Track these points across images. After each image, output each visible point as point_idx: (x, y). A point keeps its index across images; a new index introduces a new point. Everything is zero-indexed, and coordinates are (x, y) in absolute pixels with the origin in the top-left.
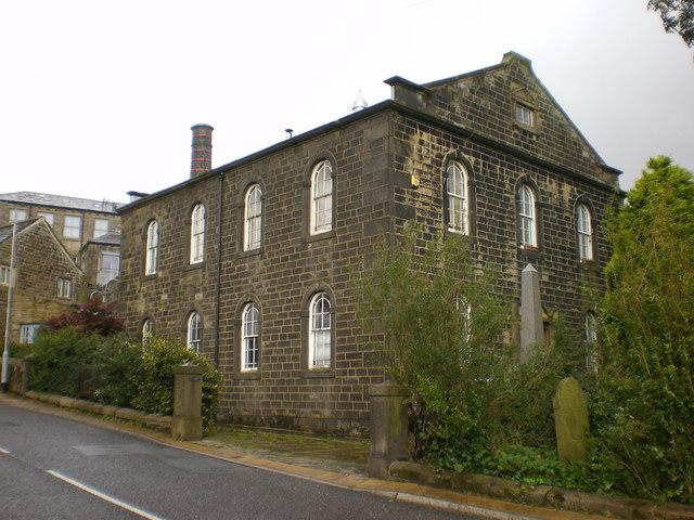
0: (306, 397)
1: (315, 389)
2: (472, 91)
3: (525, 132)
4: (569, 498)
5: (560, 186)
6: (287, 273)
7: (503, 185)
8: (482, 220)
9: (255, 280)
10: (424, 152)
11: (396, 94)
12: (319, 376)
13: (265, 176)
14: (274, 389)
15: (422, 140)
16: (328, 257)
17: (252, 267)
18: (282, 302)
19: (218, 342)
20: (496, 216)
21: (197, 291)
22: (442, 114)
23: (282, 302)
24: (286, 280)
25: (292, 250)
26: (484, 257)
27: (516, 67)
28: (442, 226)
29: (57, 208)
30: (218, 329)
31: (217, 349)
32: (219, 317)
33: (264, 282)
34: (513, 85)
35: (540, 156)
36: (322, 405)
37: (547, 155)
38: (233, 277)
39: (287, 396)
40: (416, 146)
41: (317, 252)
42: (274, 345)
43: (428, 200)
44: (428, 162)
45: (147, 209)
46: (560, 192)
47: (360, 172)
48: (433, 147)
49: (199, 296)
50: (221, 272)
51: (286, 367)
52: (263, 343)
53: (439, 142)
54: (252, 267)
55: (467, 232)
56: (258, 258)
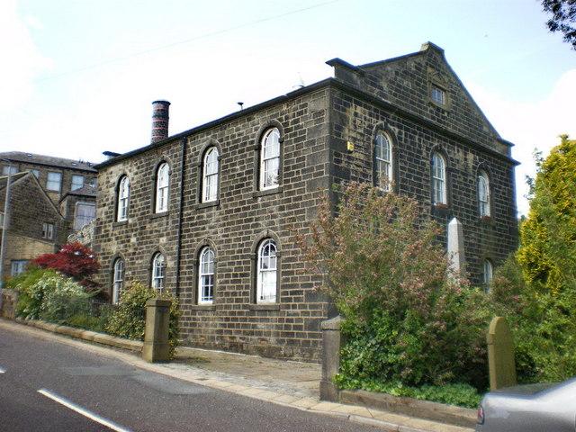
0: (254, 326)
1: (262, 320)
2: (397, 73)
3: (438, 109)
5: (465, 154)
6: (240, 222)
7: (421, 152)
8: (404, 181)
9: (211, 228)
10: (358, 122)
11: (337, 72)
12: (266, 310)
13: (221, 140)
14: (227, 319)
15: (356, 112)
16: (274, 208)
18: (234, 246)
19: (179, 279)
20: (415, 178)
21: (162, 236)
23: (234, 246)
25: (243, 203)
27: (433, 55)
30: (179, 268)
32: (180, 258)
34: (430, 70)
35: (450, 129)
36: (269, 334)
37: (455, 128)
38: (192, 225)
40: (351, 117)
41: (264, 205)
42: (227, 282)
43: (360, 163)
44: (361, 131)
45: (120, 166)
46: (466, 159)
47: (304, 138)
48: (365, 119)
49: (163, 240)
50: (182, 220)
51: (237, 300)
52: (218, 281)
56: (214, 211)
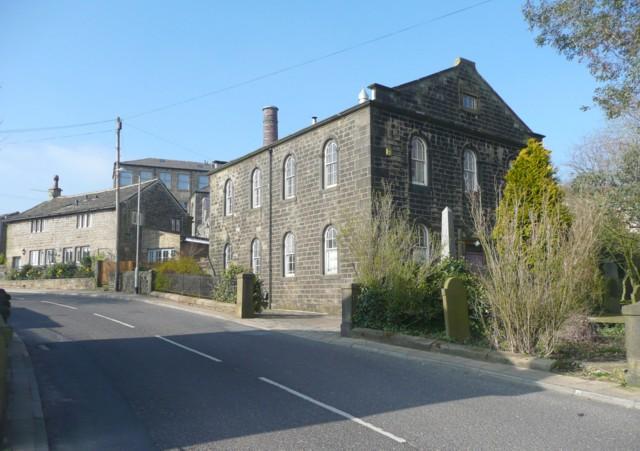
0: (323, 292)
1: (328, 286)
2: (430, 89)
4: (443, 346)
6: (311, 213)
7: (452, 151)
8: (436, 175)
9: (292, 218)
10: (395, 132)
12: (332, 279)
14: (305, 287)
16: (335, 202)
17: (290, 209)
18: (308, 232)
19: (271, 258)
20: (448, 172)
21: (258, 226)
22: (407, 106)
24: (311, 218)
25: (313, 198)
26: (438, 200)
28: (408, 180)
29: (173, 169)
31: (270, 262)
32: (271, 242)
33: (297, 219)
36: (333, 297)
38: (279, 216)
39: (312, 291)
40: (389, 129)
41: (328, 200)
42: (303, 259)
43: (397, 164)
44: (398, 139)
47: (352, 148)
48: (401, 129)
49: (259, 229)
51: (312, 273)
53: (406, 125)
54: (290, 209)
55: (426, 184)
